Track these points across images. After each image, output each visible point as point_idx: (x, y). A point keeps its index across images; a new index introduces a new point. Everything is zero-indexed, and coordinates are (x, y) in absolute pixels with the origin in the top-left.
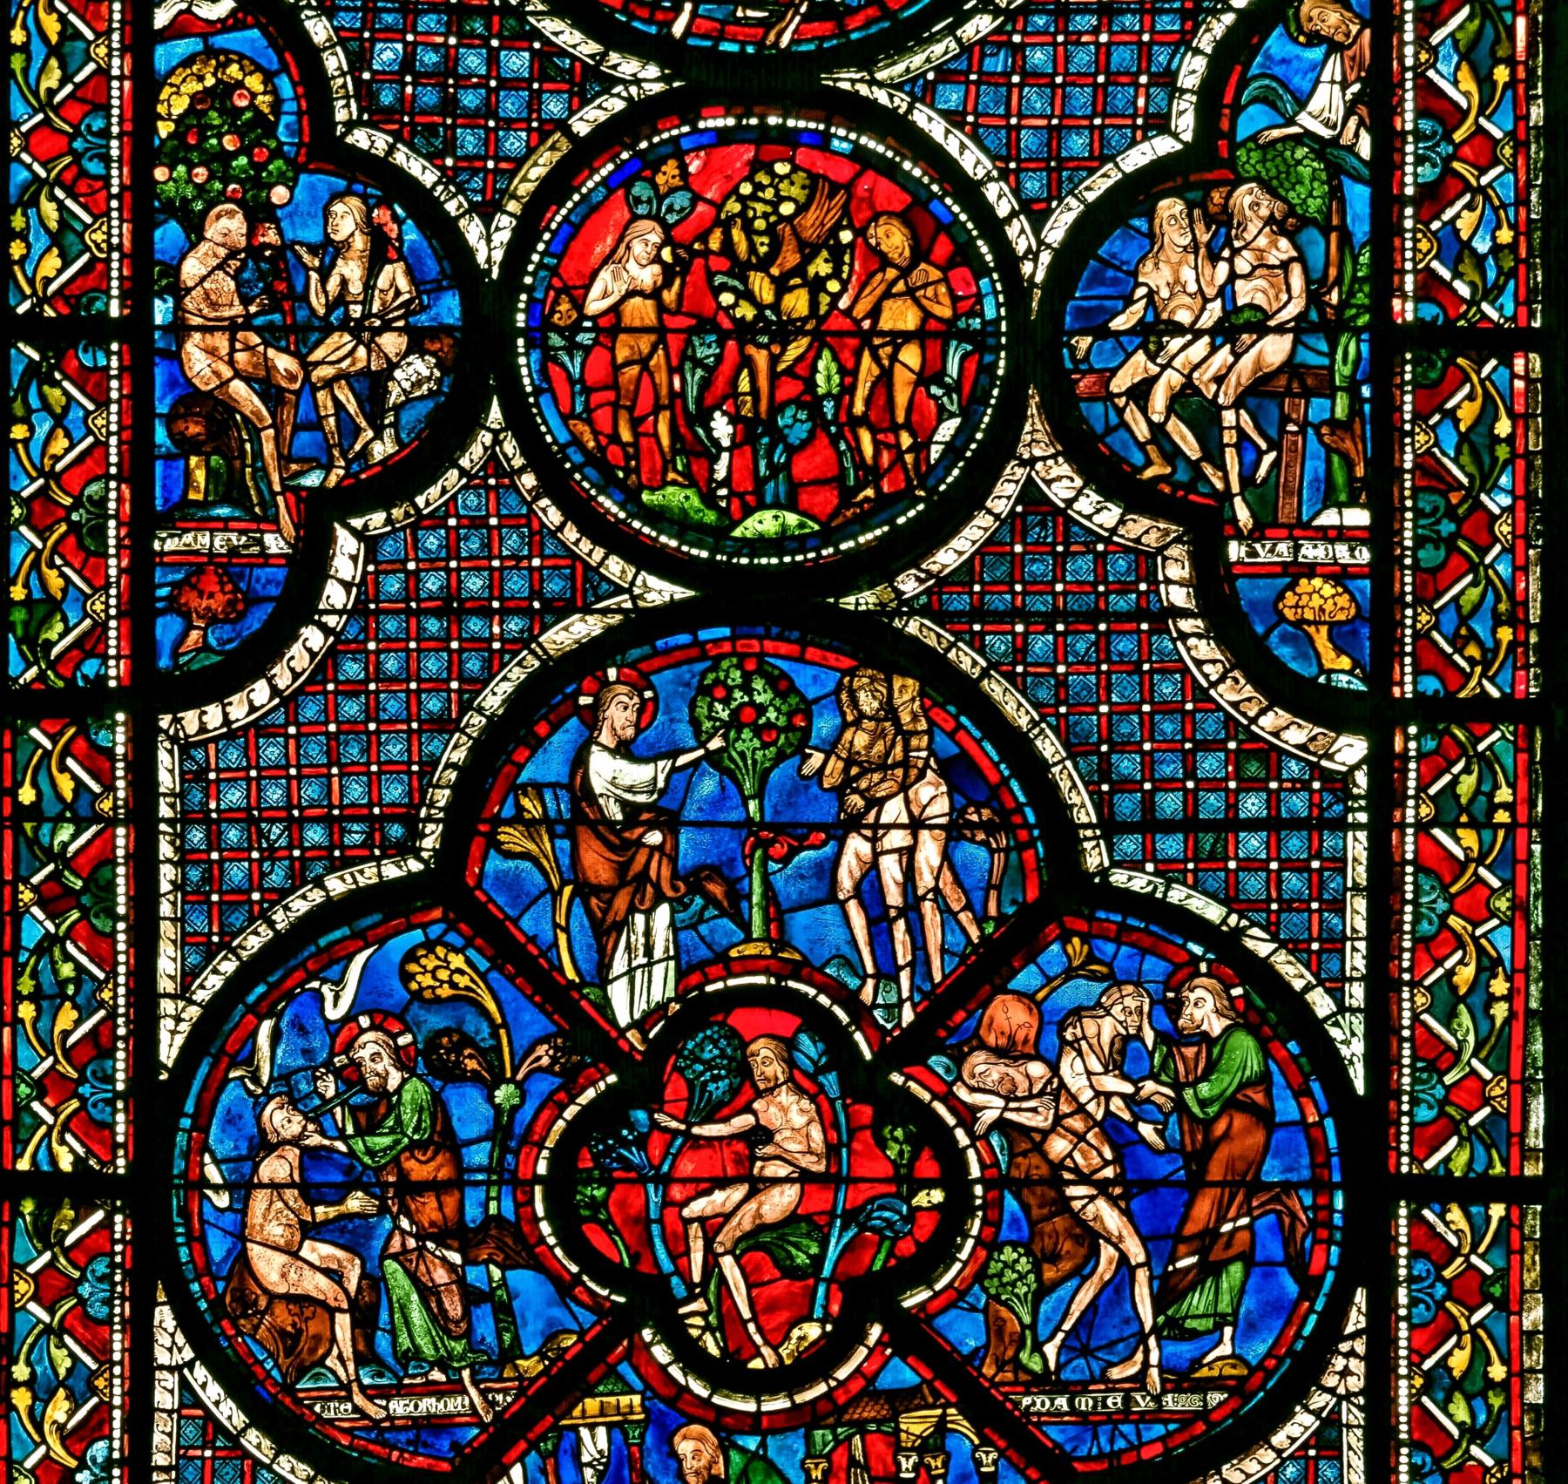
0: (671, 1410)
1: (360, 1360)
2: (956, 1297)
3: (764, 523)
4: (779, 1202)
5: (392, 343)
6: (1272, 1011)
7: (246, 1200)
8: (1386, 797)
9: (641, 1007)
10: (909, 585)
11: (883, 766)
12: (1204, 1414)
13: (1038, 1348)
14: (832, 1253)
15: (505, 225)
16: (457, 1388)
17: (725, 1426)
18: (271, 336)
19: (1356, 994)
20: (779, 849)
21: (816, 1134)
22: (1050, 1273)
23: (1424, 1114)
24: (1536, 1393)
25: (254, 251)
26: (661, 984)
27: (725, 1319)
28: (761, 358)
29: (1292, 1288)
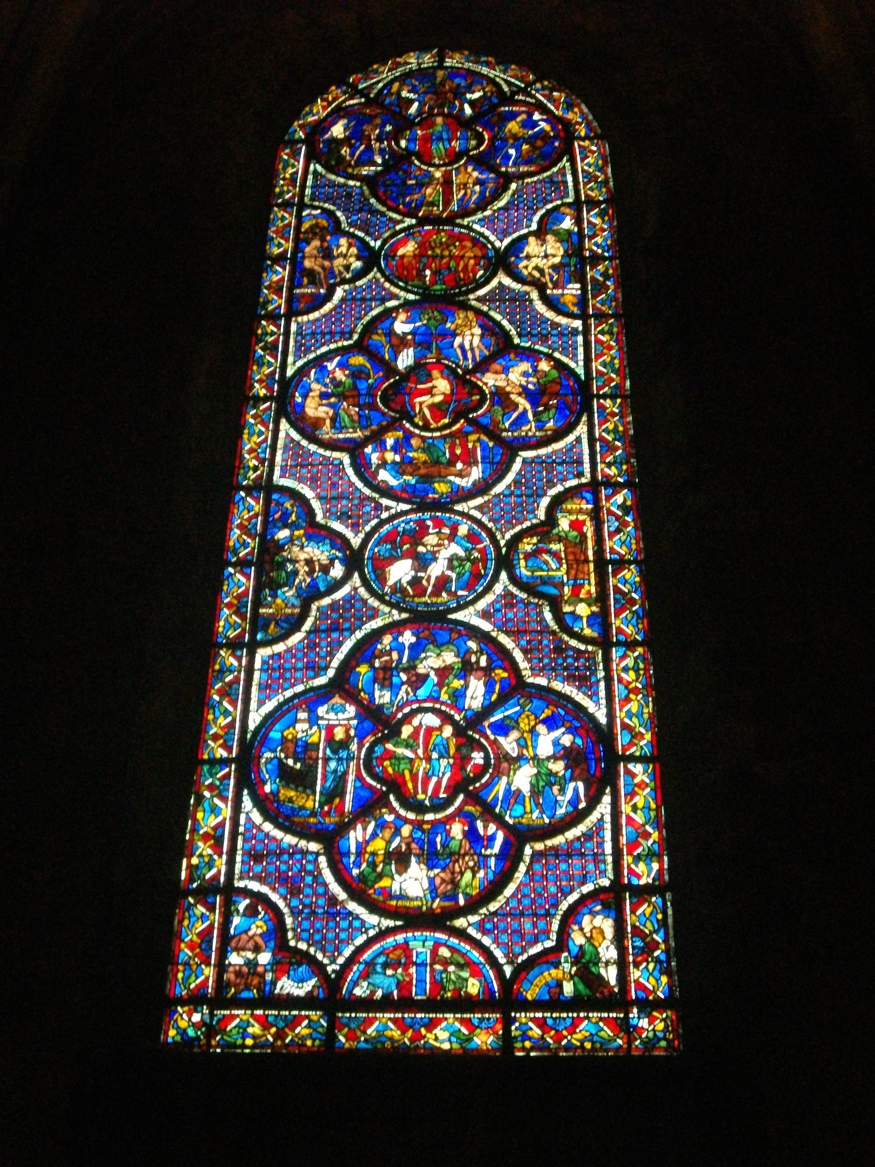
0: (409, 436)
1: (331, 428)
2: (483, 415)
3: (438, 287)
4: (438, 399)
5: (352, 260)
6: (560, 366)
7: (305, 400)
8: (586, 332)
9: (405, 366)
10: (471, 297)
11: (465, 326)
12: (546, 435)
13: (503, 423)
14: (452, 407)
15: (379, 243)
16: (356, 432)
17: (424, 439)
18: (324, 258)
19: (581, 363)
20: (440, 339)
21: (448, 387)
22: (507, 411)
23: (600, 384)
24: (632, 432)
25: (321, 246)
26: (410, 361)
27: (424, 418)
28: (438, 262)
29: (568, 413)
